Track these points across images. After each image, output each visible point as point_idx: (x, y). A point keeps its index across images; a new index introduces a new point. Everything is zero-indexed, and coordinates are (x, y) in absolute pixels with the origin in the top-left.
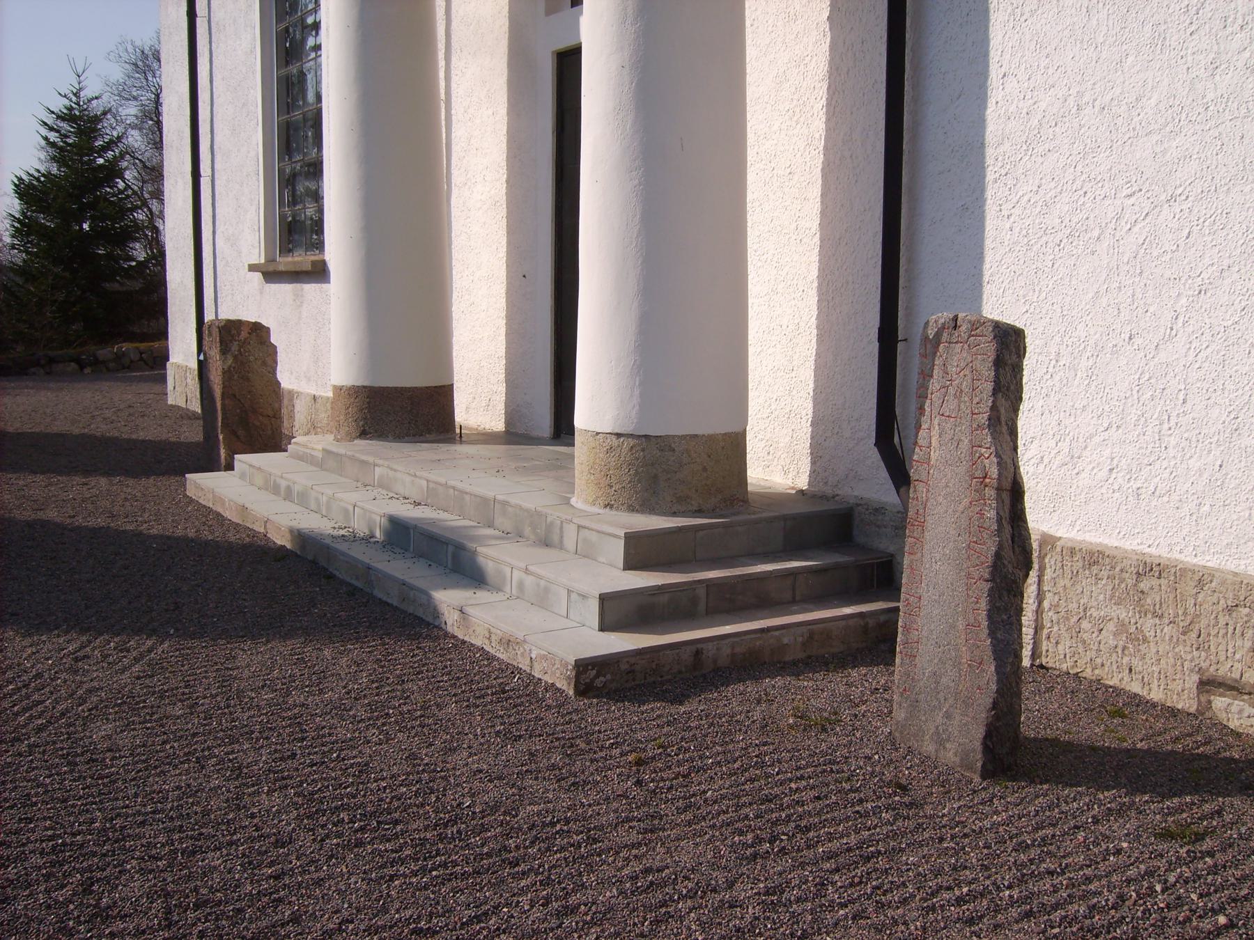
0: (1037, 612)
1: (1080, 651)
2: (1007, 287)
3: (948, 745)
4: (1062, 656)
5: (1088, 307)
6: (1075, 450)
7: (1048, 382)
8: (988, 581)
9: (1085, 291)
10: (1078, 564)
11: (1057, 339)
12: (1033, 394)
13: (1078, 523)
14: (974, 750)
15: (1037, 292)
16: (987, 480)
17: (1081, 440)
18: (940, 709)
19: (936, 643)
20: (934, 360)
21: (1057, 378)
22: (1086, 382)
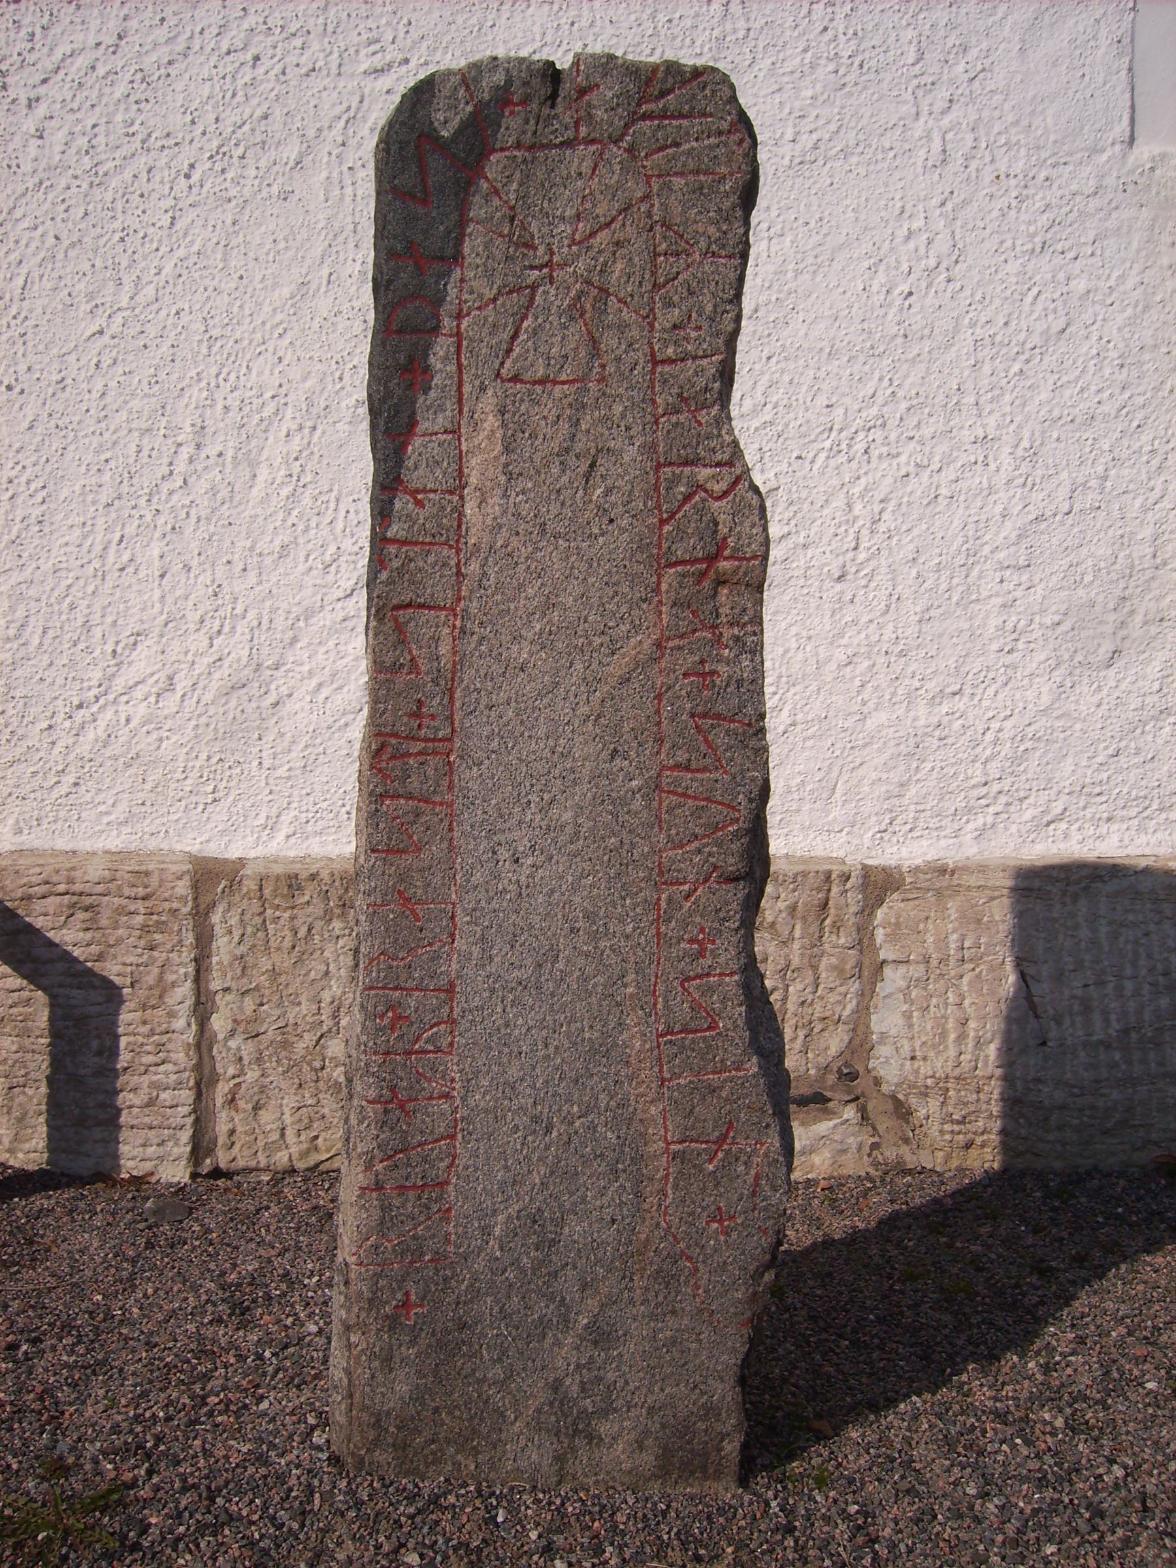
0: (198, 1046)
1: (326, 1111)
2: (36, 274)
3: (605, 1428)
4: (275, 1136)
5: (279, 317)
6: (266, 650)
7: (175, 497)
8: (736, 879)
9: (269, 283)
10: (310, 909)
11: (196, 394)
12: (130, 530)
13: (286, 818)
14: (710, 1411)
15: (128, 287)
16: (724, 565)
17: (280, 622)
18: (566, 1322)
19: (536, 1119)
20: (463, 207)
21: (200, 487)
22: (285, 491)
